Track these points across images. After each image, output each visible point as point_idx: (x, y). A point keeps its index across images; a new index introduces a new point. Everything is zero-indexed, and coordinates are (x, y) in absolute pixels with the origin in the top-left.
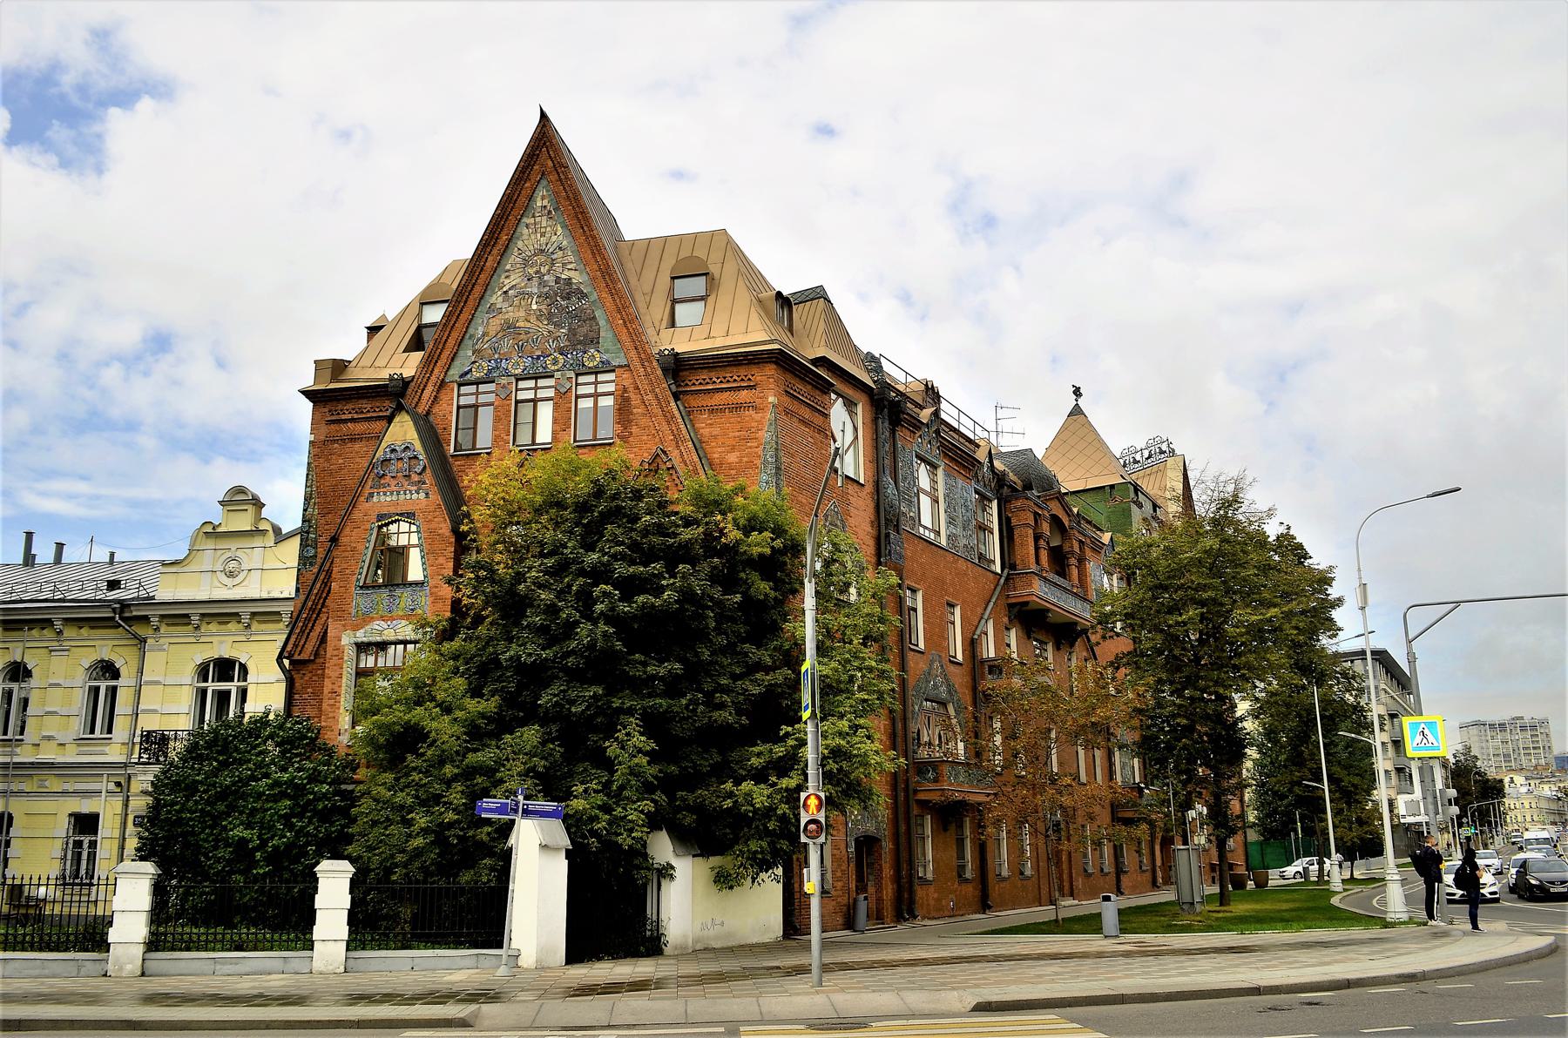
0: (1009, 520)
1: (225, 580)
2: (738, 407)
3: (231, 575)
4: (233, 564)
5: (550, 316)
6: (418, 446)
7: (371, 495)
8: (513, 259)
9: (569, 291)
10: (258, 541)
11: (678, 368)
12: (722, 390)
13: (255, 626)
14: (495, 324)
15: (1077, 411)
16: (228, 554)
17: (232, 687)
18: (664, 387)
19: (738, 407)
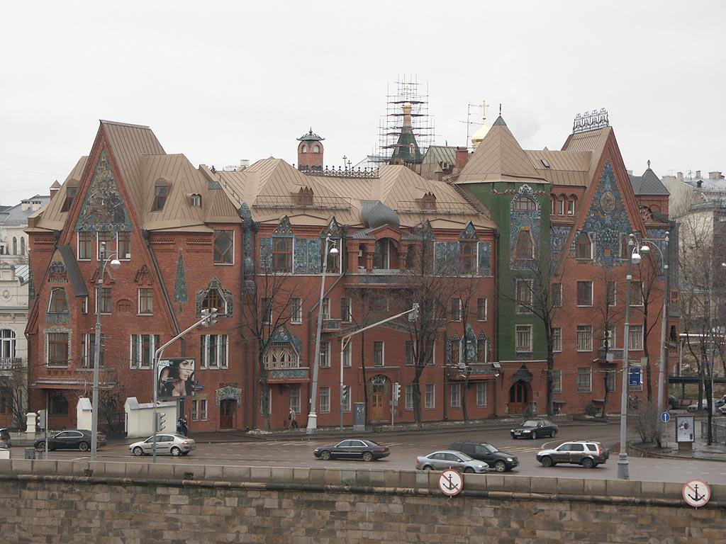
0: (346, 248)
1: (5, 300)
2: (170, 251)
3: (6, 297)
4: (6, 293)
5: (108, 209)
6: (64, 263)
7: (49, 281)
8: (95, 183)
9: (114, 199)
10: (14, 284)
11: (149, 235)
12: (164, 244)
13: (16, 318)
14: (90, 208)
15: (500, 122)
16: (4, 289)
17: (10, 339)
18: (145, 243)
19: (170, 251)
